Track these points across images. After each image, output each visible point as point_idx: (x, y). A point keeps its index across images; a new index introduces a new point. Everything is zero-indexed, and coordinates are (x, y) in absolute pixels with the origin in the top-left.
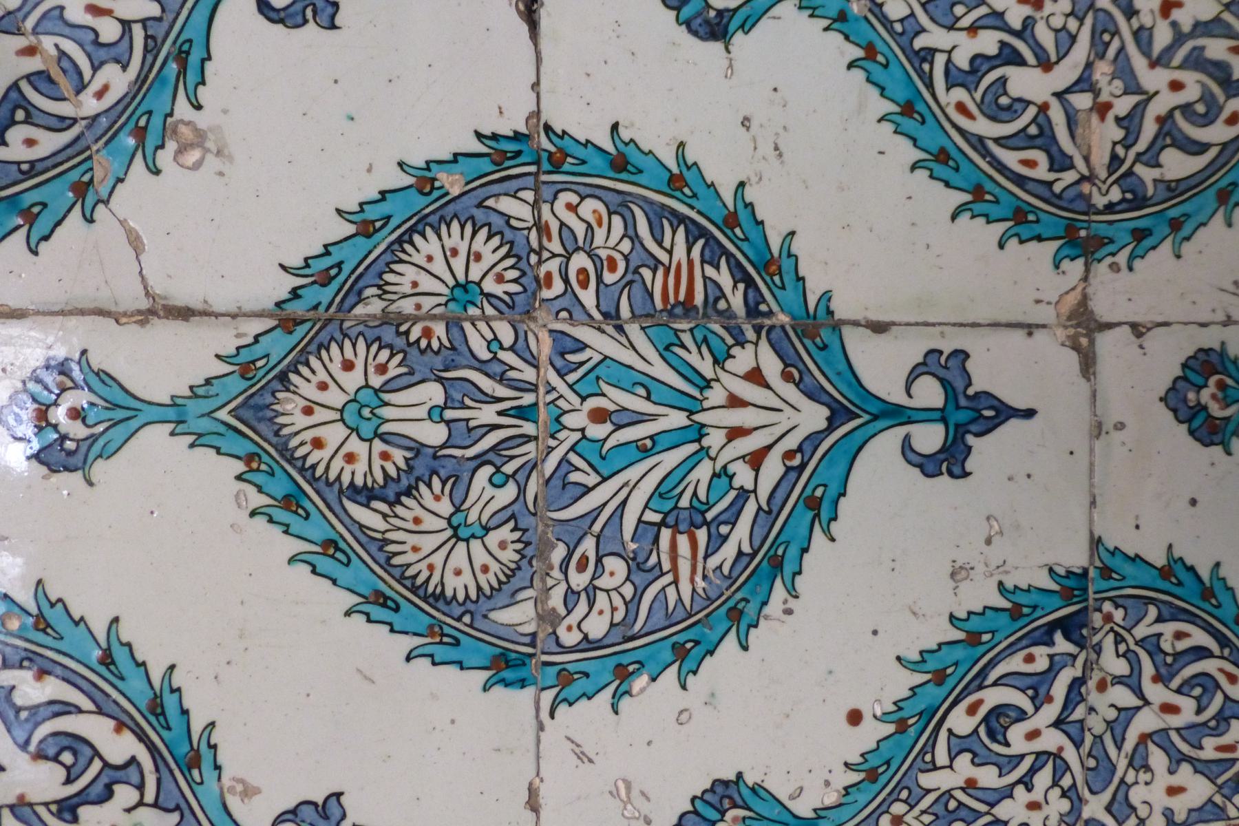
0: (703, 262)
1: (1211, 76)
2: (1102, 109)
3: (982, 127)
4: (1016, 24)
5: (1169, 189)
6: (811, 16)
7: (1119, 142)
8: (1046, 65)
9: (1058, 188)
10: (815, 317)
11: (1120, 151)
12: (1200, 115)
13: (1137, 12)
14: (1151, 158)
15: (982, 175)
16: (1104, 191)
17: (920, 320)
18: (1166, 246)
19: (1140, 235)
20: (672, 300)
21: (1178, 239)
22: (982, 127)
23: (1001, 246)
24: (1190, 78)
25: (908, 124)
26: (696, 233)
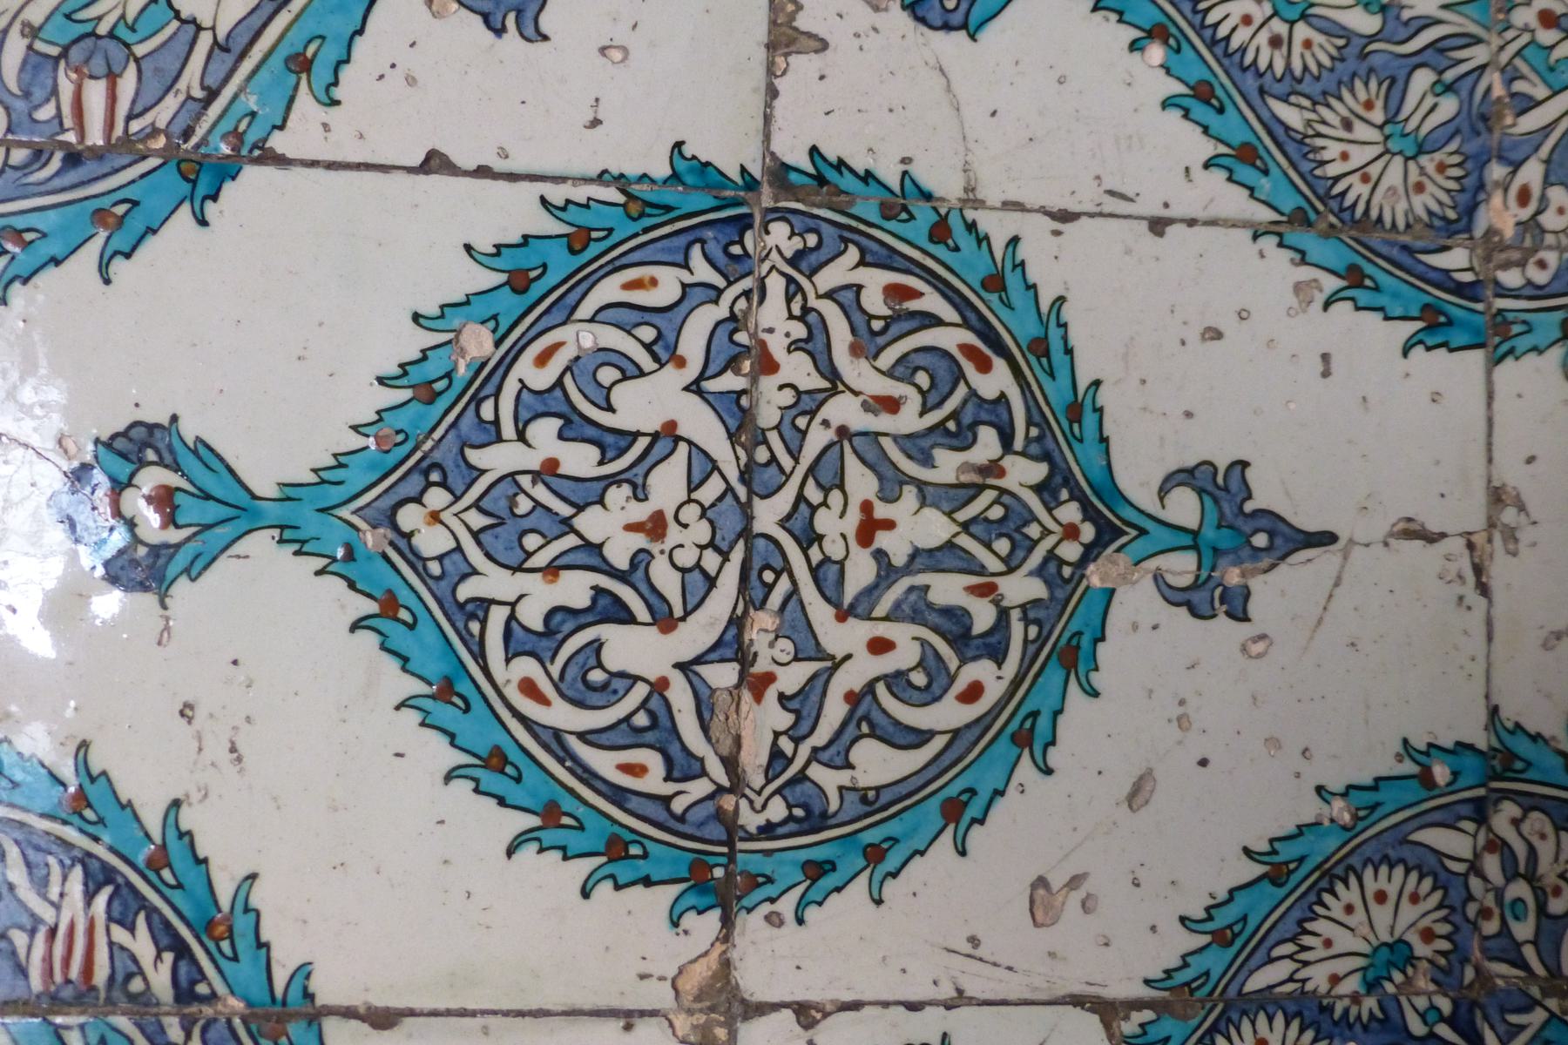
0: (110, 919)
1: (936, 630)
2: (760, 685)
3: (561, 715)
4: (622, 563)
5: (864, 800)
6: (296, 553)
7: (785, 733)
8: (665, 621)
9: (678, 806)
10: (284, 1003)
11: (786, 745)
12: (918, 688)
13: (820, 538)
14: (837, 754)
15: (558, 788)
16: (758, 806)
17: (453, 1005)
18: (860, 885)
19: (816, 870)
20: (58, 977)
21: (878, 877)
22: (561, 715)
23: (586, 894)
24: (904, 635)
25: (446, 714)
26: (101, 877)
